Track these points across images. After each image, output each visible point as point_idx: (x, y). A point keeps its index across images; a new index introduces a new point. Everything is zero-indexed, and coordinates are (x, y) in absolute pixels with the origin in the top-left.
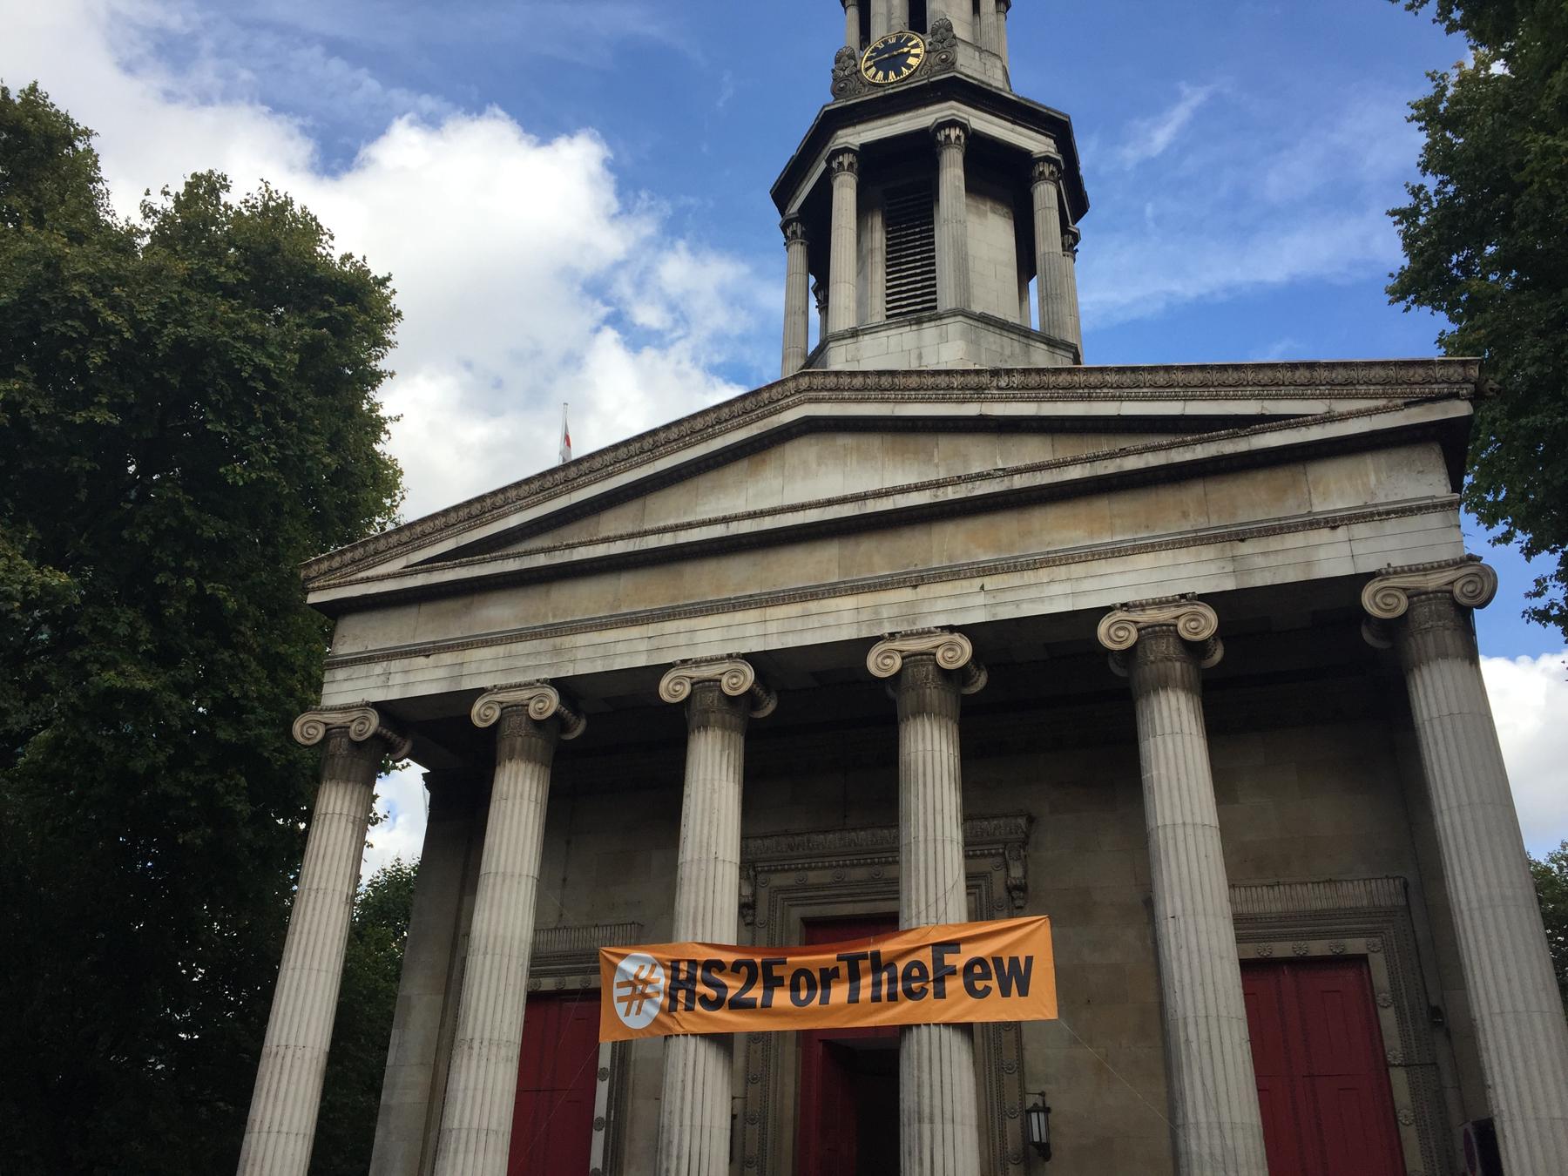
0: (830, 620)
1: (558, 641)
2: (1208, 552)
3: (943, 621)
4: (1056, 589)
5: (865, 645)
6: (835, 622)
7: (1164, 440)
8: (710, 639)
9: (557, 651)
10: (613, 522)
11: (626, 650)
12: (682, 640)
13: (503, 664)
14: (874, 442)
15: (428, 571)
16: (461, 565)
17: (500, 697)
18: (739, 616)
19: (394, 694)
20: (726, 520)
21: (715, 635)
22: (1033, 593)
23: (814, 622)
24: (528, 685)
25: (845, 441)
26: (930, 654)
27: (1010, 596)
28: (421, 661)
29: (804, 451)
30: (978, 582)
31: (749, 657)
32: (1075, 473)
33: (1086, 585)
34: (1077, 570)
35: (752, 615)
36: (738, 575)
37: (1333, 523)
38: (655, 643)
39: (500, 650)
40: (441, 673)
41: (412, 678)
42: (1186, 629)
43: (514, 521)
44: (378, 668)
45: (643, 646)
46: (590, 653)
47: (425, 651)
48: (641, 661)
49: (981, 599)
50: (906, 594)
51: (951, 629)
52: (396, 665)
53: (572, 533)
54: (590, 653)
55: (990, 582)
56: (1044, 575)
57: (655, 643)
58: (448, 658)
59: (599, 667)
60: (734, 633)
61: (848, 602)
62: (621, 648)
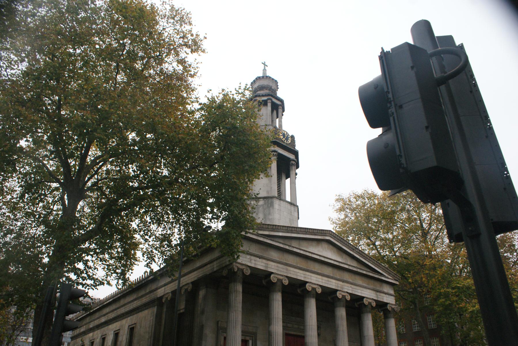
0: (332, 283)
1: (287, 267)
2: (374, 292)
3: (346, 290)
4: (359, 291)
5: (336, 291)
6: (332, 284)
7: (369, 270)
8: (316, 280)
9: (287, 269)
10: (294, 243)
11: (300, 275)
12: (309, 277)
13: (276, 268)
14: (335, 249)
15: (264, 238)
16: (271, 240)
17: (276, 276)
18: (318, 276)
19: (253, 265)
20: (320, 256)
21: (315, 279)
22: (357, 290)
23: (329, 283)
24: (282, 275)
25: (331, 246)
26: (345, 296)
27: (354, 290)
28: (258, 259)
29: (325, 245)
30: (351, 285)
31: (320, 286)
32: (364, 272)
33: (363, 292)
34: (362, 289)
35: (320, 277)
36: (317, 267)
37: (386, 293)
38: (305, 276)
39: (276, 264)
40: (264, 265)
41: (257, 263)
42: (372, 304)
43: (281, 234)
44: (248, 257)
45: (303, 275)
46: (293, 273)
47: (260, 257)
48: (302, 279)
49: (351, 289)
50: (341, 283)
51: (347, 292)
52: (253, 257)
53: (287, 242)
54: (293, 273)
55: (352, 286)
56: (358, 288)
57: (305, 276)
58: (264, 261)
59: (295, 277)
60: (318, 279)
61: (334, 281)
62: (299, 274)
